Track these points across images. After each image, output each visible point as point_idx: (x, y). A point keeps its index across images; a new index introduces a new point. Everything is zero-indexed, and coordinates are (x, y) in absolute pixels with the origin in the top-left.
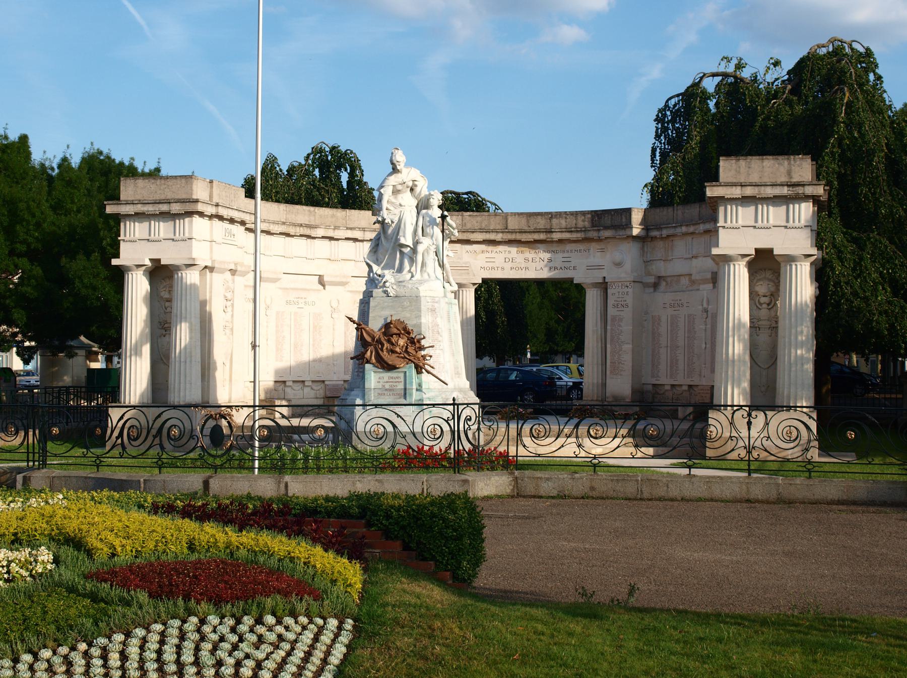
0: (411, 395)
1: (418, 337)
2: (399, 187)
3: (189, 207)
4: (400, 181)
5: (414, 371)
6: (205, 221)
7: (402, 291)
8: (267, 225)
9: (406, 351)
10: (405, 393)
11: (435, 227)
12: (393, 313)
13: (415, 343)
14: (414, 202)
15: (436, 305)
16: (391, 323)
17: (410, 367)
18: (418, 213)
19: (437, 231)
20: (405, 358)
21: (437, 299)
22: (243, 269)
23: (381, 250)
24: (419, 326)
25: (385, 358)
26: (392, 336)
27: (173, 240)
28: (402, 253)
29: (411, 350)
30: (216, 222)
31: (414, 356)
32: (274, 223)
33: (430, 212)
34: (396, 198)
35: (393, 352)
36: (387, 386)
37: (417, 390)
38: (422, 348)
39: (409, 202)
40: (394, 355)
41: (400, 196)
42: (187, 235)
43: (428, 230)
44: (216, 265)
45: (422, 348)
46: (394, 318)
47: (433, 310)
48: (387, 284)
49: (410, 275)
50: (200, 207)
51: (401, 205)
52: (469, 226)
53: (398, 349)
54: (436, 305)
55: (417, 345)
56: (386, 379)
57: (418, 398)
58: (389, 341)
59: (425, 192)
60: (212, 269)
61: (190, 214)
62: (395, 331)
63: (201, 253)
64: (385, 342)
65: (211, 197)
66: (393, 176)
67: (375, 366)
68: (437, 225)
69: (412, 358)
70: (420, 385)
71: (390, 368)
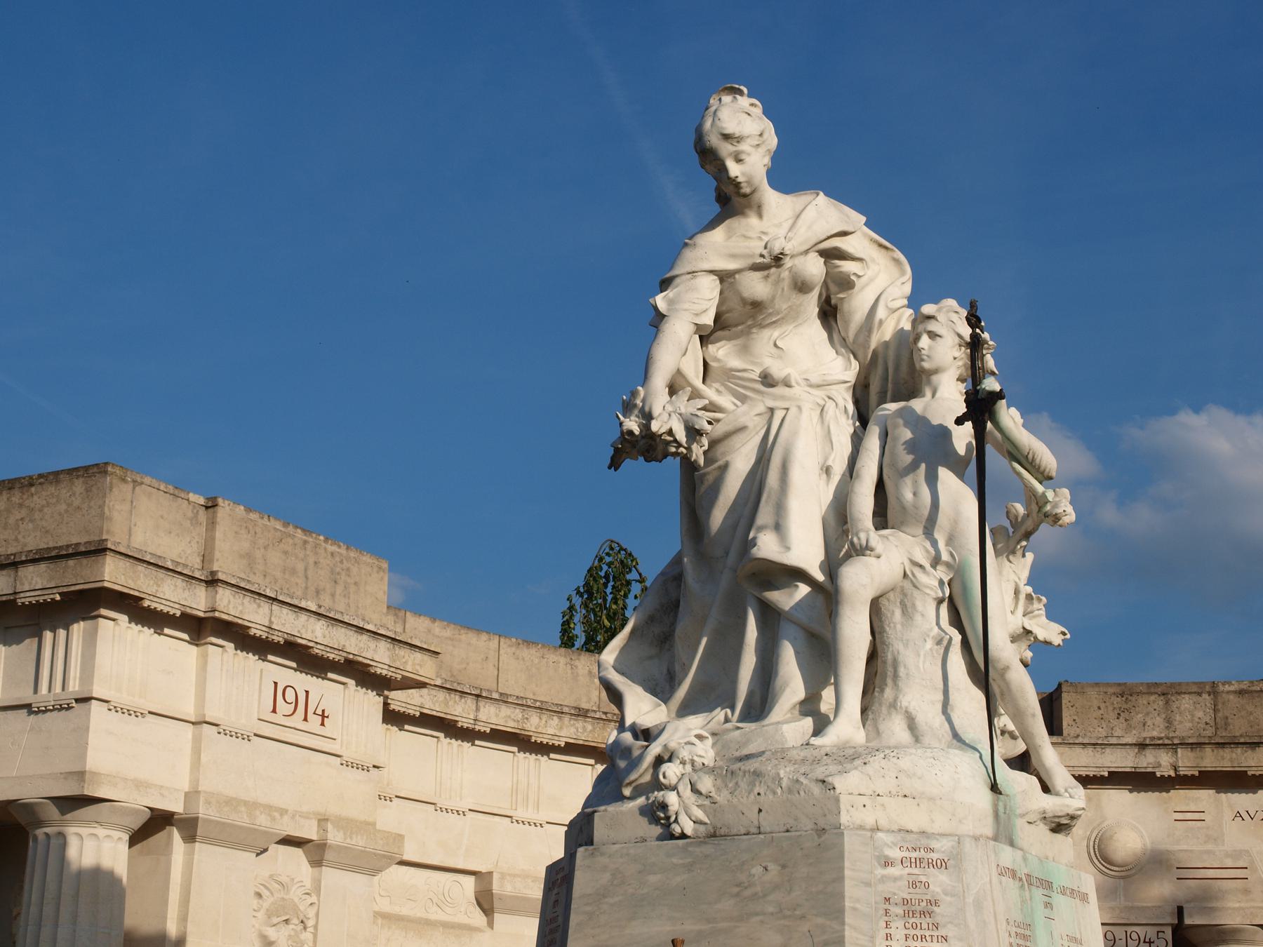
2: (755, 286)
3: (77, 576)
4: (758, 247)
6: (173, 649)
7: (742, 806)
8: (518, 713)
11: (946, 477)
14: (844, 370)
15: (939, 881)
18: (863, 419)
19: (957, 496)
21: (942, 847)
22: (359, 841)
23: (683, 626)
27: (28, 707)
28: (770, 617)
30: (222, 654)
32: (542, 709)
33: (917, 405)
34: (745, 350)
39: (811, 362)
41: (764, 339)
42: (74, 686)
43: (911, 491)
44: (203, 811)
48: (671, 771)
49: (808, 722)
50: (114, 574)
51: (767, 380)
52: (1239, 728)
54: (939, 881)
59: (894, 320)
60: (190, 828)
61: (88, 602)
63: (131, 759)
65: (206, 557)
66: (718, 234)
68: (958, 466)
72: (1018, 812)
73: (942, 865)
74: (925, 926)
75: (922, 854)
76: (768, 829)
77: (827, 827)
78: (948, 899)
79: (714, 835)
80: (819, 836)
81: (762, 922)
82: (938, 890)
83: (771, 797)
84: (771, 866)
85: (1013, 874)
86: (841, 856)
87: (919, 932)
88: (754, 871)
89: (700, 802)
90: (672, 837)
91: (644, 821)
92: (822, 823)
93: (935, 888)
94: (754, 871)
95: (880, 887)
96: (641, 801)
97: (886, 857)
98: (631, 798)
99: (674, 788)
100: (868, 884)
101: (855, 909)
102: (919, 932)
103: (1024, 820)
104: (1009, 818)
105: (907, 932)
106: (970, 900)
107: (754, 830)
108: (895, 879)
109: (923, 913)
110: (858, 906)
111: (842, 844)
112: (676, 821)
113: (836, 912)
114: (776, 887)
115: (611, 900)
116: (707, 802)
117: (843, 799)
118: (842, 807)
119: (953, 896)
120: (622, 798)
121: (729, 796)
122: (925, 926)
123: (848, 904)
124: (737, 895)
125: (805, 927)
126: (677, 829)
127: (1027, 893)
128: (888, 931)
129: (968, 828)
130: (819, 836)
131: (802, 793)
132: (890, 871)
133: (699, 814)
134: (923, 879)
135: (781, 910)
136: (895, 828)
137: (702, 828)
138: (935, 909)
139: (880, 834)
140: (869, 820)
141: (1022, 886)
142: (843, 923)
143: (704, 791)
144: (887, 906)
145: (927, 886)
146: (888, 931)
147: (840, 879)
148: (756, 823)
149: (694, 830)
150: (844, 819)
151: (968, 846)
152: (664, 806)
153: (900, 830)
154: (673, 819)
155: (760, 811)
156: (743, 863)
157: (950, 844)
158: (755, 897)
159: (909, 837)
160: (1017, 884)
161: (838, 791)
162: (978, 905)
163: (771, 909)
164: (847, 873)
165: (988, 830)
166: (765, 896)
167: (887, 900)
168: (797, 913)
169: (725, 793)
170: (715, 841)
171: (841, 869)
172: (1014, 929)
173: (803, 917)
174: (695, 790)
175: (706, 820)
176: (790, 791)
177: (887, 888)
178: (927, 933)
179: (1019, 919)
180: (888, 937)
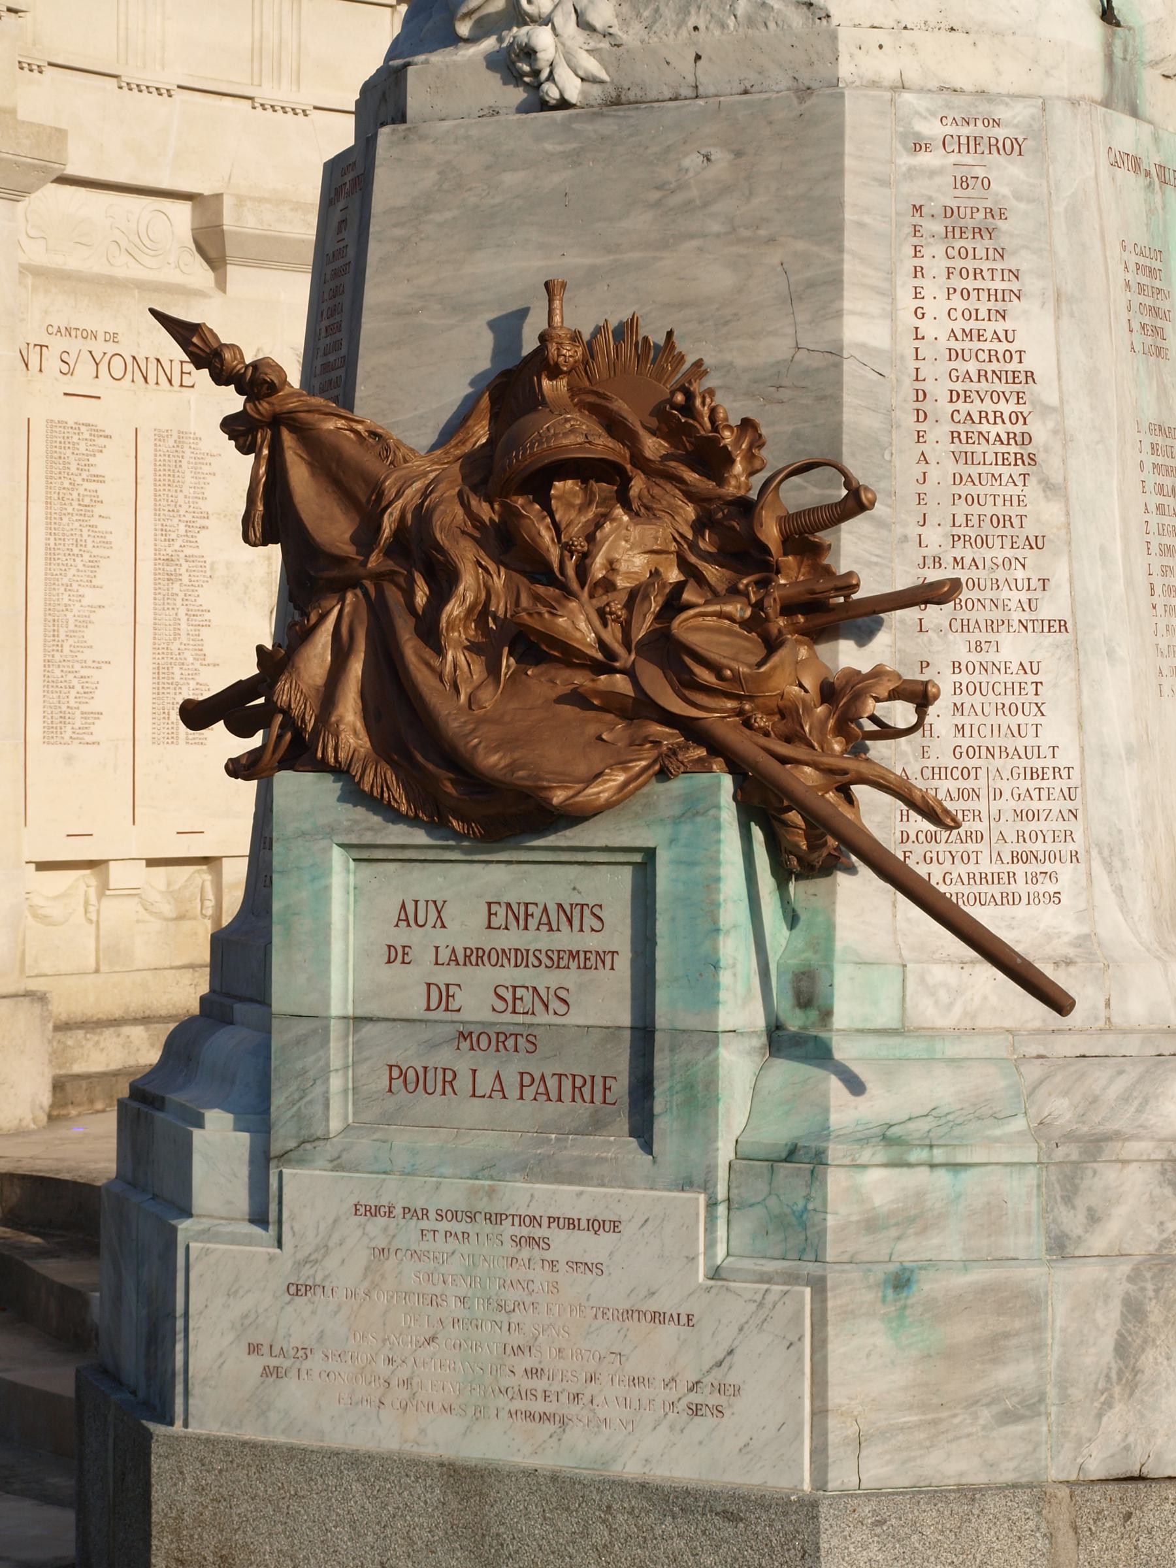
0: (701, 1097)
1: (802, 494)
5: (731, 852)
9: (667, 650)
10: (642, 1085)
12: (570, 261)
13: (775, 557)
15: (1007, 176)
16: (541, 362)
17: (697, 809)
20: (642, 708)
24: (819, 379)
25: (450, 713)
26: (538, 483)
29: (710, 628)
31: (735, 688)
35: (534, 647)
36: (476, 997)
37: (779, 1040)
38: (837, 611)
40: (546, 683)
45: (837, 611)
46: (582, 315)
47: (972, 228)
53: (579, 625)
54: (1007, 176)
55: (790, 577)
56: (465, 928)
57: (777, 1133)
58: (507, 544)
62: (577, 434)
64: (467, 557)
67: (355, 794)
69: (716, 714)
70: (810, 991)
71: (499, 813)
72: (1148, 57)
73: (1014, 148)
74: (981, 253)
75: (980, 129)
76: (712, 90)
77: (814, 85)
78: (1022, 206)
79: (616, 102)
80: (802, 100)
81: (700, 249)
82: (1005, 191)
83: (717, 33)
84: (717, 154)
85: (1136, 164)
86: (839, 135)
87: (970, 264)
88: (686, 162)
89: (593, 44)
90: (544, 106)
91: (494, 79)
92: (806, 78)
93: (1000, 188)
94: (686, 162)
95: (906, 188)
96: (489, 44)
97: (917, 135)
98: (471, 40)
99: (547, 21)
100: (884, 183)
101: (861, 225)
102: (970, 264)
103: (1157, 72)
104: (1131, 69)
105: (950, 263)
106: (1060, 208)
107: (686, 91)
108: (933, 173)
109: (978, 232)
110: (867, 219)
111: (841, 114)
112: (551, 77)
113: (832, 234)
114: (726, 190)
115: (437, 217)
116: (605, 45)
117: (844, 34)
118: (842, 47)
119: (1030, 201)
120: (455, 40)
121: (644, 33)
122: (981, 253)
123: (849, 216)
124: (658, 204)
125: (775, 257)
126: (552, 92)
127: (1158, 198)
128: (917, 262)
129: (1059, 84)
130: (802, 100)
131: (772, 25)
132: (924, 159)
133: (592, 65)
134: (980, 172)
135: (734, 229)
136: (933, 84)
137: (596, 91)
138: (1000, 223)
139: (907, 97)
140: (887, 68)
141: (1150, 184)
142: (840, 250)
143: (599, 25)
144: (917, 220)
145: (986, 184)
146: (917, 262)
147: (836, 173)
148: (690, 79)
149: (583, 93)
150: (845, 69)
151: (1059, 113)
152: (529, 53)
153: (941, 89)
154: (545, 74)
155: (698, 57)
156: (668, 150)
157: (1033, 110)
158: (688, 207)
159: (958, 100)
160: (1142, 181)
161: (834, 21)
162: (1074, 216)
163: (716, 227)
164: (849, 162)
165: (1095, 88)
166: (705, 205)
167: (918, 209)
168: (762, 232)
169: (637, 28)
170: (620, 111)
171: (840, 155)
172: (1135, 259)
173: (771, 240)
174: (583, 24)
175: (604, 76)
176: (751, 22)
177: (916, 190)
178: (985, 266)
179: (1143, 241)
180: (918, 272)
